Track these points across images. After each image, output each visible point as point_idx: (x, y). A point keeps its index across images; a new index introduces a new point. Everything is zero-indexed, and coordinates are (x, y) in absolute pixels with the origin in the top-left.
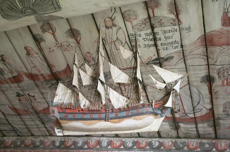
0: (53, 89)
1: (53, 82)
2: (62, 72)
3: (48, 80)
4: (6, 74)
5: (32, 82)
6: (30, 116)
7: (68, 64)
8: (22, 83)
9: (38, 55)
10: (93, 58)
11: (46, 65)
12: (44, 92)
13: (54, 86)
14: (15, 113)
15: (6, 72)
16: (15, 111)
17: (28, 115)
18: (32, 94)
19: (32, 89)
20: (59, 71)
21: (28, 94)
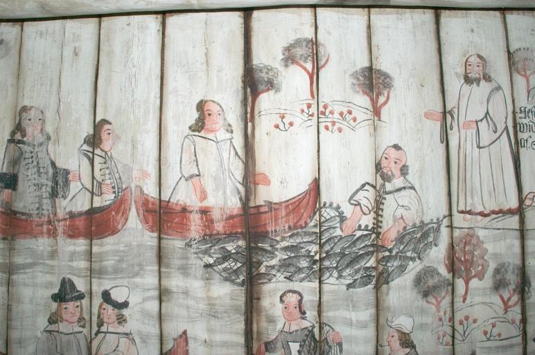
1: (231, 247)
2: (284, 205)
3: (218, 234)
4: (69, 198)
5: (150, 239)
7: (316, 184)
8: (110, 240)
9: (228, 135)
10: (404, 166)
11: (239, 174)
12: (175, 290)
15: (74, 187)
20: (275, 200)
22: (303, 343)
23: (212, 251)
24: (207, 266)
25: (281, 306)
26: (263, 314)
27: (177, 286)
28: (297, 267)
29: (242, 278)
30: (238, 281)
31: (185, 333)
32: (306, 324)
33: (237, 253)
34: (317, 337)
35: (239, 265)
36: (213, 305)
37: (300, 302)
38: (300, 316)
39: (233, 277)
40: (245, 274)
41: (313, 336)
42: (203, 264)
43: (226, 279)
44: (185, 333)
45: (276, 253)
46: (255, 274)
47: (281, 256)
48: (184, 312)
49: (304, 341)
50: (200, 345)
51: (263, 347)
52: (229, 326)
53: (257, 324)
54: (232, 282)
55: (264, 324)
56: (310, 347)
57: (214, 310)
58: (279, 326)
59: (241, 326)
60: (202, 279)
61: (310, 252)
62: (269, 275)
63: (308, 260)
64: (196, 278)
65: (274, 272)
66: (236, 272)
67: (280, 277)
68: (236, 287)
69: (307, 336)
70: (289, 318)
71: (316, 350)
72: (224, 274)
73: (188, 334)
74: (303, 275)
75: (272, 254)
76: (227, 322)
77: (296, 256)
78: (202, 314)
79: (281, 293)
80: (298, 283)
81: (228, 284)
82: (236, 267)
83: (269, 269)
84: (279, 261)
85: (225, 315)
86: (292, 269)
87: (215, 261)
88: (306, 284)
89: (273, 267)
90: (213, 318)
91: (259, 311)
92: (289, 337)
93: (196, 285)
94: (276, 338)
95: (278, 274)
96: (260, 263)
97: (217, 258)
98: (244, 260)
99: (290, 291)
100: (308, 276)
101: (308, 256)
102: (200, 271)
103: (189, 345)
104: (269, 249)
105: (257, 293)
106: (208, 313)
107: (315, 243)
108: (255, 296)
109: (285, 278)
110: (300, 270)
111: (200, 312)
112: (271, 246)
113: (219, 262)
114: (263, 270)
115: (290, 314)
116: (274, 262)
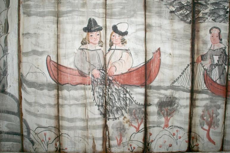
0: (177, 18)
6: (85, 89)
12: (154, 25)
13: (181, 12)
14: (50, 80)
16: (55, 73)
17: (81, 89)
18: (122, 28)
19: (132, 13)
21: (115, 29)
22: (220, 56)
23: (174, 4)
24: (172, 12)
25: (210, 35)
26: (201, 39)
27: (155, 23)
28: (218, 14)
29: (190, 19)
30: (188, 21)
31: (159, 49)
32: (222, 46)
33: (187, 5)
34: (227, 54)
35: (188, 12)
36: (175, 34)
37: (219, 33)
38: (219, 41)
39: (185, 19)
40: (191, 17)
41: (225, 53)
42: (169, 11)
43: (182, 20)
44: (159, 49)
45: (208, 6)
46: (196, 17)
47: (210, 8)
48: (159, 38)
49: (221, 55)
50: (167, 56)
51: (200, 58)
52: (183, 46)
53: (197, 45)
54: (185, 21)
55: (201, 45)
56: (223, 58)
57: (175, 37)
58: (209, 46)
59: (189, 46)
60: (169, 19)
61: (225, 6)
62: (204, 18)
63: (224, 11)
64: (166, 18)
65: (207, 16)
66: (187, 16)
67: (210, 19)
68: (187, 24)
69: (222, 52)
70: (214, 43)
71: (226, 61)
72: (181, 17)
73: (161, 50)
74: (221, 19)
75: (206, 6)
76: (182, 43)
77: (218, 8)
78: (168, 39)
79: (210, 28)
80: (219, 23)
81: (182, 22)
82: (186, 13)
83: (204, 15)
84: (210, 10)
85: (181, 39)
86: (216, 15)
87: (176, 10)
88: (222, 24)
89: (206, 14)
90: (175, 41)
91: (198, 38)
92: (214, 53)
93: (166, 22)
94: (207, 53)
95: (209, 18)
96: (199, 12)
97: (177, 8)
98: (191, 10)
99: (215, 27)
100: (224, 20)
101: (224, 9)
102: (168, 15)
103: (162, 56)
104: (204, 3)
105: (198, 28)
106: (172, 38)
107: (227, 2)
108: (196, 29)
109: (212, 20)
110: (220, 16)
111: (168, 37)
112: (205, 2)
113: (178, 10)
114: (201, 15)
115: (214, 40)
116: (207, 11)
